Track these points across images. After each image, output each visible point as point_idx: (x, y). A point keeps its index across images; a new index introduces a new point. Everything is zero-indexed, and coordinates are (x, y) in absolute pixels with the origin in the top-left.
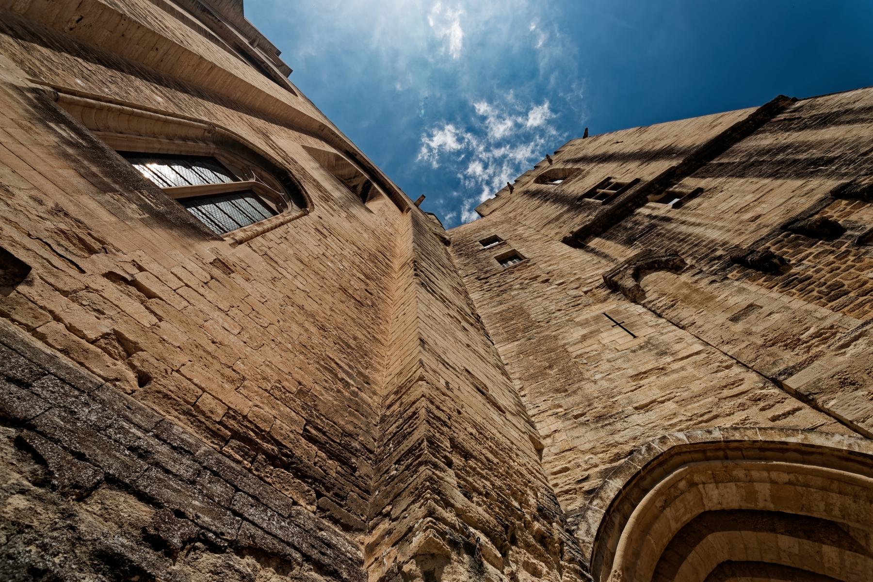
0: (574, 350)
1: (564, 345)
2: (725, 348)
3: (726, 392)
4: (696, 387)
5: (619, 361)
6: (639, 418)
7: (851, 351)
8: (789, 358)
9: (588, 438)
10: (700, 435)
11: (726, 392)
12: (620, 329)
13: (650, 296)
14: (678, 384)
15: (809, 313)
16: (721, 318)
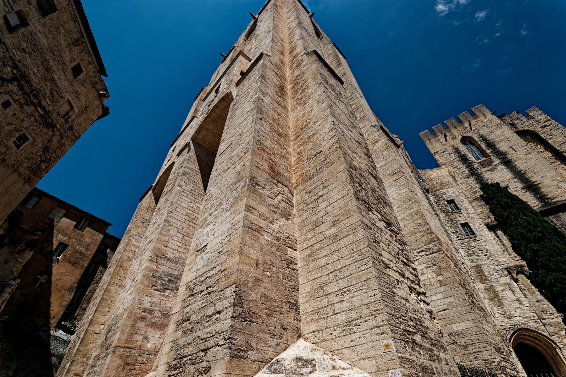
0: (501, 294)
1: (497, 291)
2: (534, 308)
3: (531, 318)
4: (527, 315)
5: (511, 303)
6: (515, 319)
7: (554, 320)
8: (544, 316)
9: (506, 320)
10: (526, 326)
11: (531, 318)
12: (511, 292)
13: (520, 283)
14: (524, 313)
15: (551, 308)
16: (534, 300)
